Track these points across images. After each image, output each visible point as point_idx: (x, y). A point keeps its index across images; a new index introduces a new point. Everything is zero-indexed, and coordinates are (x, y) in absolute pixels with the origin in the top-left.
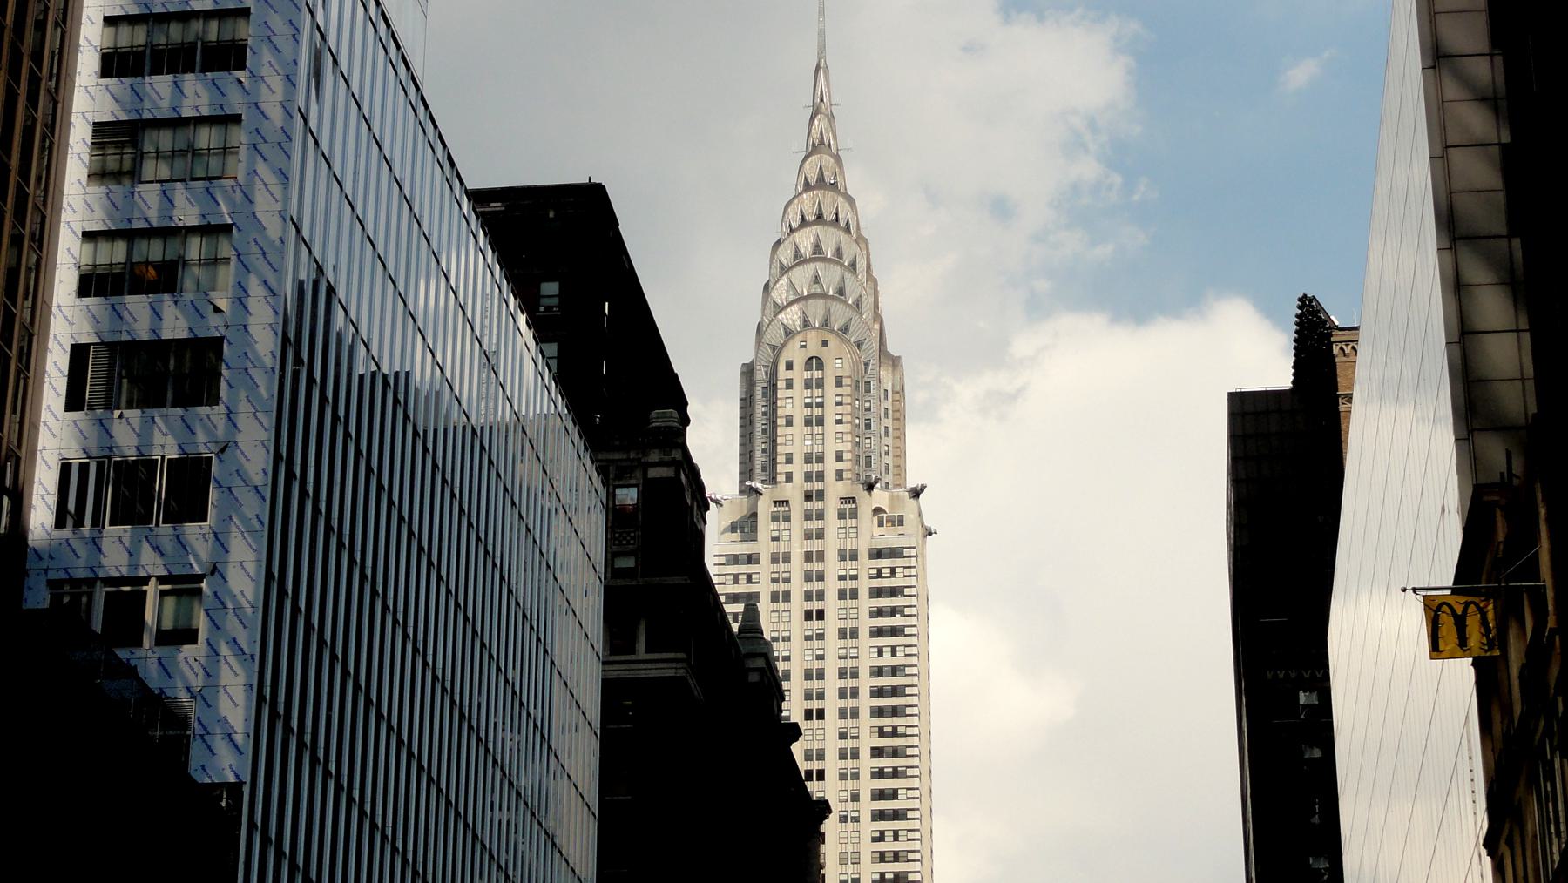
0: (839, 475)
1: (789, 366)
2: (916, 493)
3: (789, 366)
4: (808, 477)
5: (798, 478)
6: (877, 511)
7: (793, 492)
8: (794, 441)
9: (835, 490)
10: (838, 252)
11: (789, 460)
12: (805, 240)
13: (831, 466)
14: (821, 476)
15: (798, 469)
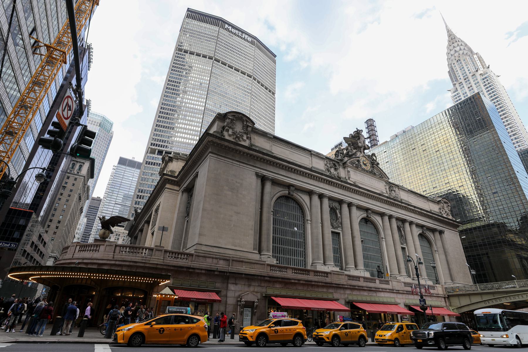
0: (470, 73)
1: (454, 64)
2: (488, 67)
3: (454, 64)
4: (464, 77)
5: (462, 78)
6: (481, 74)
7: (462, 80)
8: (459, 73)
9: (470, 76)
10: (458, 45)
11: (459, 76)
12: (451, 48)
13: (468, 72)
14: (466, 75)
15: (462, 77)
